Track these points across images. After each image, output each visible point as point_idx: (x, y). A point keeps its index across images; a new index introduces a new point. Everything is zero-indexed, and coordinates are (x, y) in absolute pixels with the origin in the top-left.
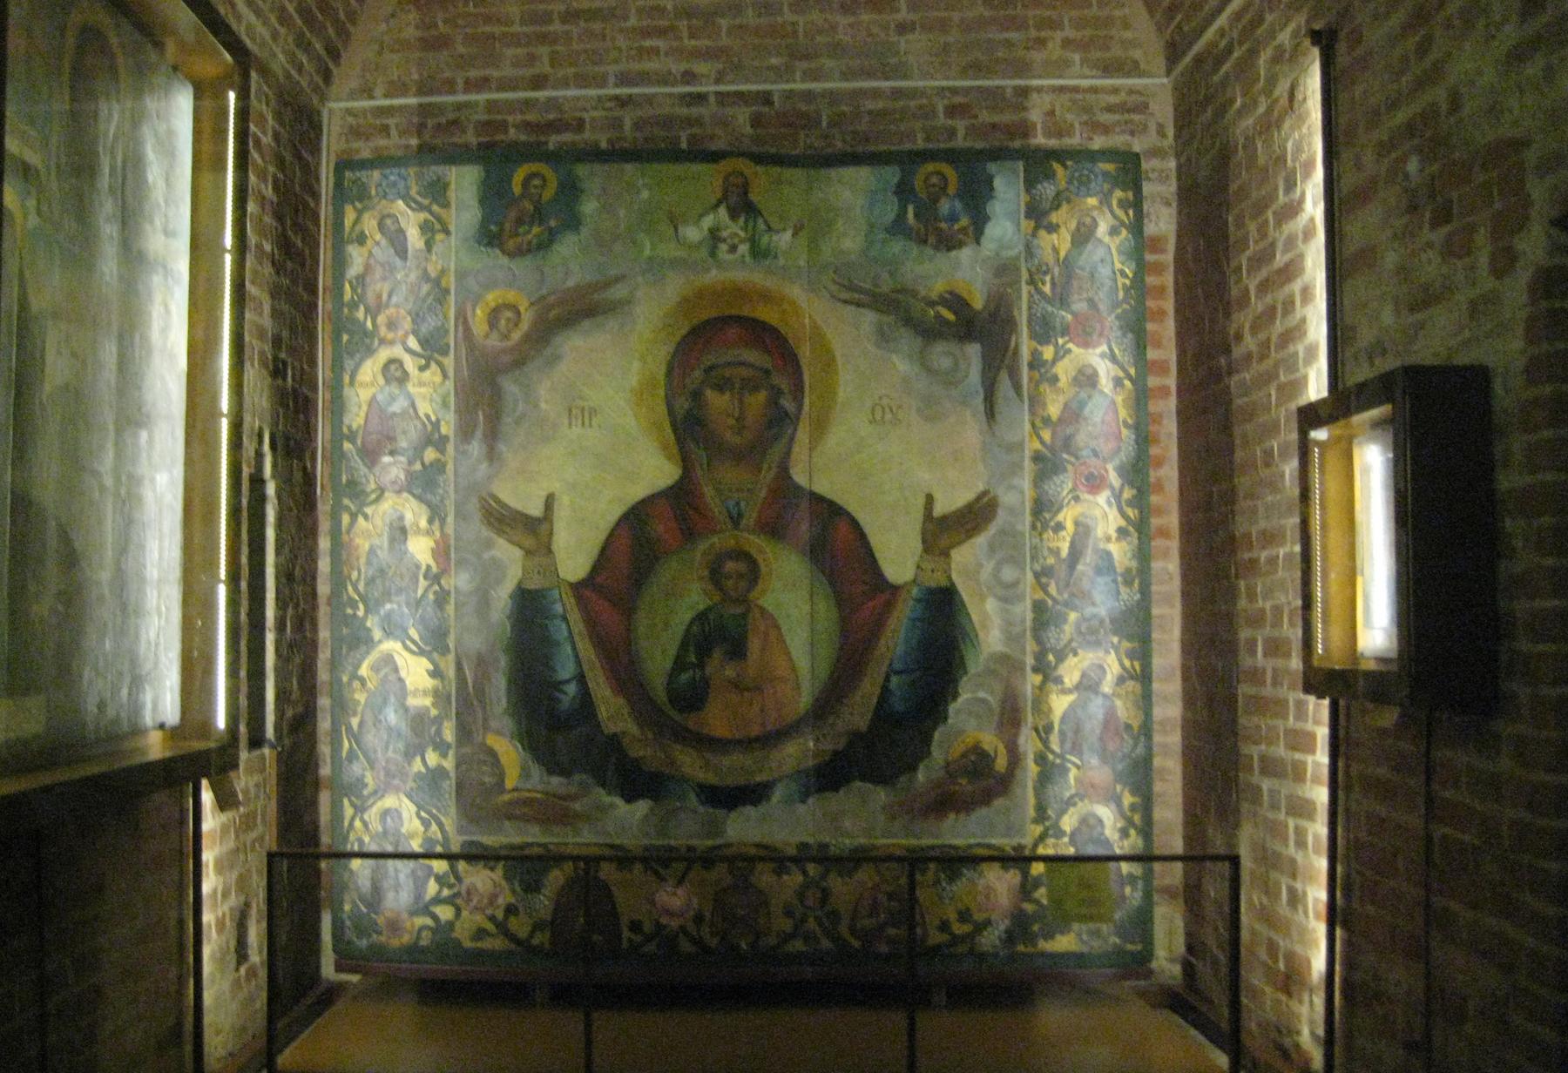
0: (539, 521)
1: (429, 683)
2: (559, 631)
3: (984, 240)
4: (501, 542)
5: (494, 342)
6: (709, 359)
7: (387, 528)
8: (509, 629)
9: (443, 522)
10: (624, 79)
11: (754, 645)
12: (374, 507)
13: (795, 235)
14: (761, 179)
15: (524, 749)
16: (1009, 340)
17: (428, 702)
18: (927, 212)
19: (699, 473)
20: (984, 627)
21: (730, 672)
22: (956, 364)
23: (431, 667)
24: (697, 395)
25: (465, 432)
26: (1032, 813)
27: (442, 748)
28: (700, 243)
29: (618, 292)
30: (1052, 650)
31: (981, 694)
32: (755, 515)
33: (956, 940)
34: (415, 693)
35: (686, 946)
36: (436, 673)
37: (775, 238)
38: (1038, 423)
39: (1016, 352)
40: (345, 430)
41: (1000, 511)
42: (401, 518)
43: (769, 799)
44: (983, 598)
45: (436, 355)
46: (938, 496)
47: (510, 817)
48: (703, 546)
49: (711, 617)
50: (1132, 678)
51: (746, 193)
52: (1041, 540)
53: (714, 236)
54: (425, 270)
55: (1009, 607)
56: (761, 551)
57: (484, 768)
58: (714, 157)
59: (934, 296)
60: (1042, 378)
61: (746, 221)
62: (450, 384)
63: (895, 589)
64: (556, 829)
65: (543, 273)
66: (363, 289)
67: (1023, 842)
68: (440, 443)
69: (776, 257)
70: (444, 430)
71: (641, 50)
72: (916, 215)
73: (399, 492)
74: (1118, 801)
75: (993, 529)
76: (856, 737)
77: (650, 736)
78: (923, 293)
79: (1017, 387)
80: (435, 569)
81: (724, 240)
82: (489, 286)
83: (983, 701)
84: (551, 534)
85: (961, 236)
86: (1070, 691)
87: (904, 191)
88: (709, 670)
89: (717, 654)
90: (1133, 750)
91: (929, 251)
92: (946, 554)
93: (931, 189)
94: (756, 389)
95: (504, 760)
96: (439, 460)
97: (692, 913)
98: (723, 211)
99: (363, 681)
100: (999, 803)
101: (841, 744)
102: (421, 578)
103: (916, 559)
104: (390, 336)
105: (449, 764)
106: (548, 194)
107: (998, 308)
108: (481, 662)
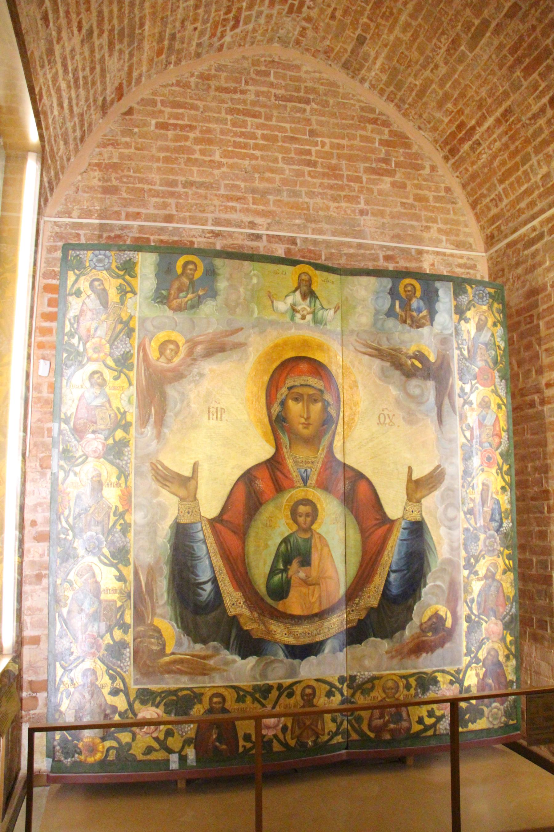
0: (188, 479)
1: (117, 585)
2: (201, 550)
3: (435, 323)
4: (164, 492)
5: (162, 363)
6: (290, 382)
7: (89, 482)
8: (169, 547)
9: (126, 478)
10: (217, 222)
11: (315, 558)
12: (80, 467)
13: (335, 312)
14: (319, 277)
15: (178, 627)
16: (449, 380)
17: (115, 597)
18: (406, 305)
19: (285, 450)
20: (439, 543)
21: (302, 574)
22: (423, 391)
23: (118, 574)
24: (283, 403)
25: (143, 421)
26: (465, 651)
27: (124, 627)
28: (286, 312)
29: (239, 338)
30: (473, 556)
31: (438, 583)
32: (315, 477)
33: (427, 728)
34: (107, 590)
35: (277, 747)
36: (121, 578)
37: (326, 313)
38: (464, 428)
39: (453, 386)
40: (63, 416)
41: (446, 476)
42: (99, 475)
43: (324, 650)
44: (438, 527)
45: (125, 370)
46: (414, 468)
47: (169, 672)
48: (287, 496)
49: (292, 540)
50: (509, 570)
51: (310, 285)
52: (467, 493)
53: (294, 309)
54: (120, 316)
55: (450, 531)
56: (319, 499)
57: (153, 640)
58: (294, 263)
59: (411, 353)
60: (465, 402)
61: (310, 302)
62: (133, 389)
63: (392, 522)
64: (200, 678)
65: (193, 322)
66: (78, 325)
67: (461, 667)
68: (126, 427)
69: (326, 324)
70: (129, 418)
71: (226, 207)
72: (400, 307)
73: (98, 458)
74: (503, 639)
75: (443, 487)
76: (371, 610)
77: (256, 615)
78: (405, 351)
79: (453, 407)
80: (121, 509)
81: (298, 312)
82: (160, 328)
83: (438, 586)
84: (196, 488)
85: (423, 321)
86: (481, 579)
87: (393, 293)
88: (290, 573)
89: (295, 564)
90: (510, 611)
91: (407, 327)
92: (419, 501)
93: (408, 293)
94: (316, 401)
95: (165, 634)
96: (125, 438)
97: (281, 725)
98: (298, 294)
99: (71, 584)
100: (447, 645)
101: (363, 615)
102: (112, 515)
103: (404, 504)
104: (95, 356)
105: (129, 638)
106: (198, 274)
107: (442, 363)
108: (152, 571)
